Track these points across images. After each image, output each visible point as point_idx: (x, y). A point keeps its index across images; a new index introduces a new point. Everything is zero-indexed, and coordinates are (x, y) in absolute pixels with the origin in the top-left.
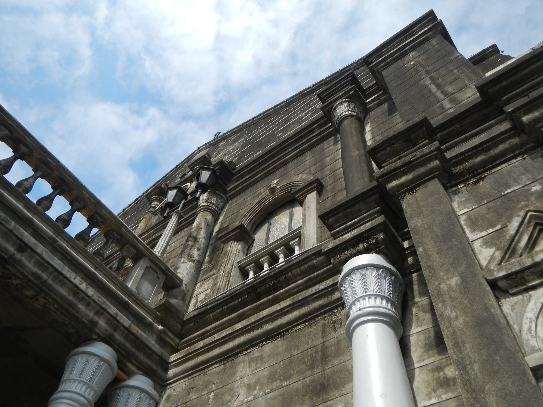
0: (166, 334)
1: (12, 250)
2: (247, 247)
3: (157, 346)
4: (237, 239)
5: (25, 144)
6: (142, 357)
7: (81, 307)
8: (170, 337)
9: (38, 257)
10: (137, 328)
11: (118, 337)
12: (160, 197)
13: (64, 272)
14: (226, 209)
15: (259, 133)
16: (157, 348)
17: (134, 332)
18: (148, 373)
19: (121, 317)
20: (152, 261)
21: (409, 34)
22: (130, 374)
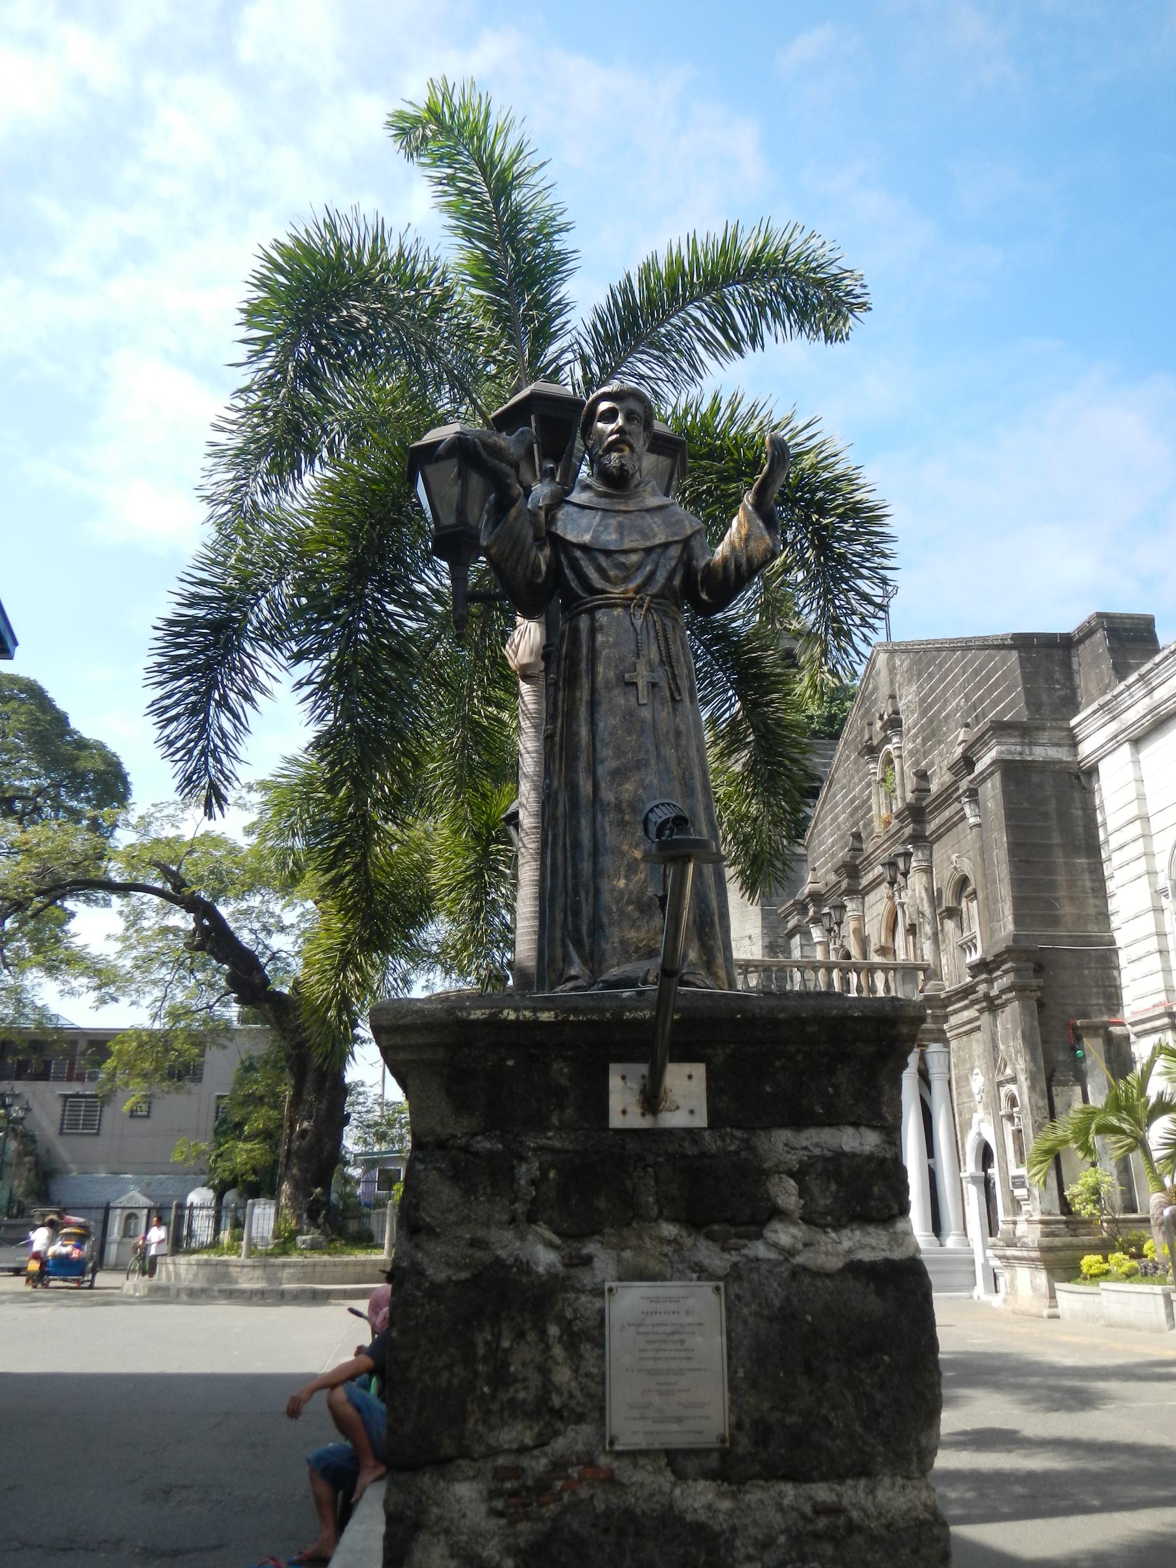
4: (950, 918)
14: (935, 856)
16: (933, 1026)
18: (936, 1041)
22: (926, 1046)
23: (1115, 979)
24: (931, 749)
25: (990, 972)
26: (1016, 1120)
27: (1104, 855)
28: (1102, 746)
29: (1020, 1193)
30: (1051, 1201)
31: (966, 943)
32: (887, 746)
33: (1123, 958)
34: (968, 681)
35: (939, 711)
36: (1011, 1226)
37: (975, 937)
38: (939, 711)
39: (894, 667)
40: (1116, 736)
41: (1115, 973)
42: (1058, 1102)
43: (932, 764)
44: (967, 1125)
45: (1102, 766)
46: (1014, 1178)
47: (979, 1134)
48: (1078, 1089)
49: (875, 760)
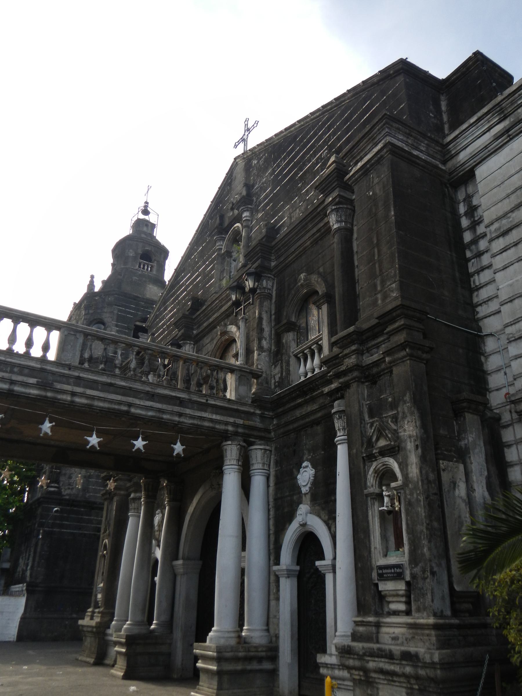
0: (264, 414)
1: (177, 419)
2: (296, 333)
3: (261, 424)
5: (148, 349)
6: (256, 433)
7: (217, 426)
8: (266, 414)
9: (189, 415)
10: (247, 422)
11: (240, 430)
12: (221, 236)
13: (203, 416)
15: (284, 169)
17: (247, 424)
19: (238, 421)
20: (240, 371)
21: (372, 137)
23: (481, 364)
24: (283, 206)
25: (362, 343)
26: (386, 499)
27: (468, 254)
28: (486, 147)
29: (387, 586)
30: (443, 598)
31: (302, 352)
32: (238, 224)
33: (490, 345)
34: (334, 133)
35: (296, 174)
36: (374, 629)
37: (321, 339)
38: (296, 174)
39: (251, 166)
40: (508, 131)
41: (483, 359)
42: (445, 477)
43: (281, 218)
44: (290, 517)
45: (480, 172)
46: (380, 568)
47: (304, 525)
48: (461, 467)
49: (223, 239)
